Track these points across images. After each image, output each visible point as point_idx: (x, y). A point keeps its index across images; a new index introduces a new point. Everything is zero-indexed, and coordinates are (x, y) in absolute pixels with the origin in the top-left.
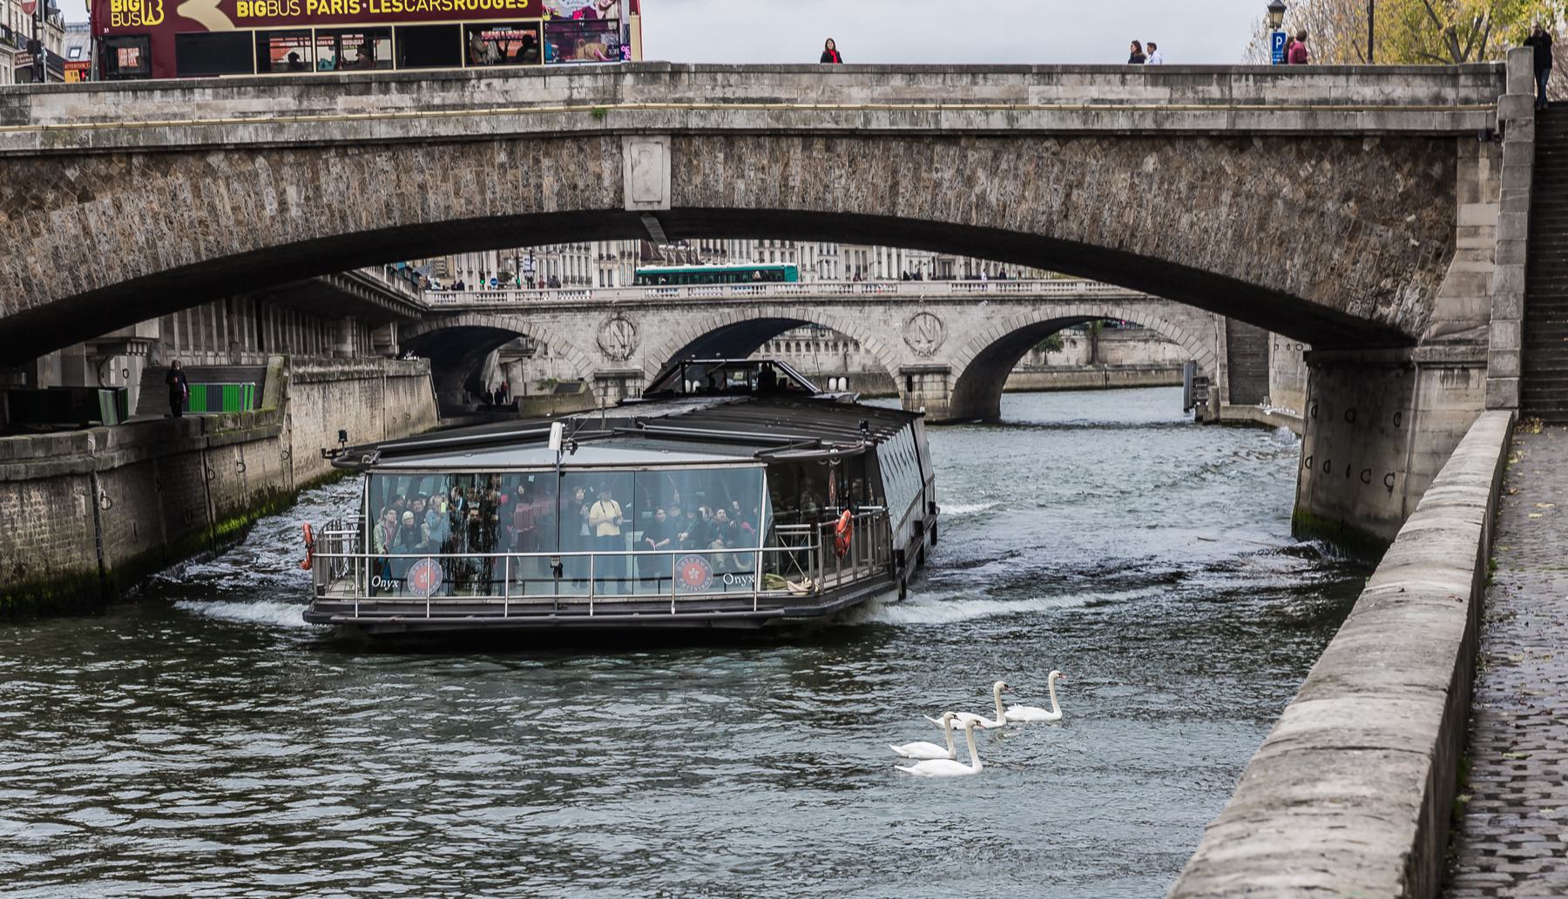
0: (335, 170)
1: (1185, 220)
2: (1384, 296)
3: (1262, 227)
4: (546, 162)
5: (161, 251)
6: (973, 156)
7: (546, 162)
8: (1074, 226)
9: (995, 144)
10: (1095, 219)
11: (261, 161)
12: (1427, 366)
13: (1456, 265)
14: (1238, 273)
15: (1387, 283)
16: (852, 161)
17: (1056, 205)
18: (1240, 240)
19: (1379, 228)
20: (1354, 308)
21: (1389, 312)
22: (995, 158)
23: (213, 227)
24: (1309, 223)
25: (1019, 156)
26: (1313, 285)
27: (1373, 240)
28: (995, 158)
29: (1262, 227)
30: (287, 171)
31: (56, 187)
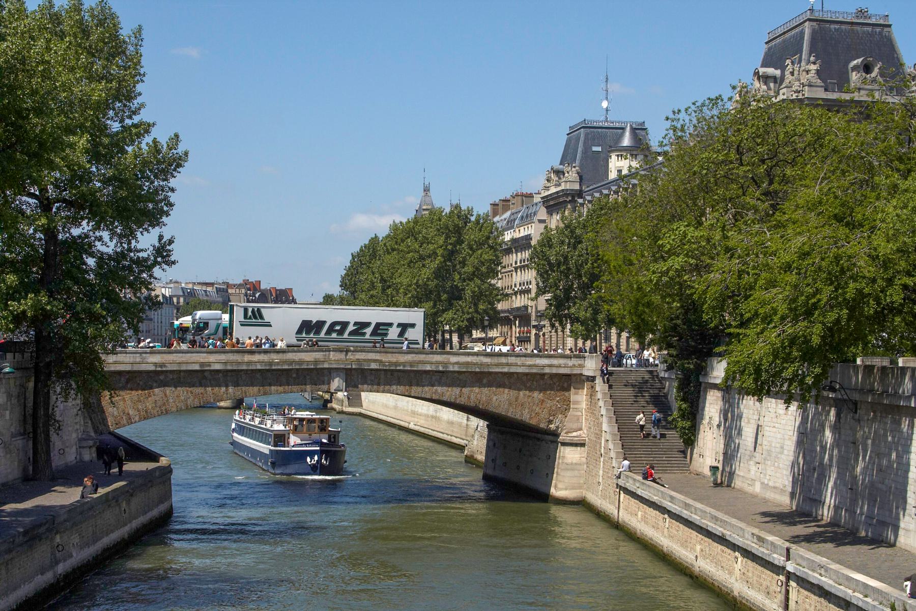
0: (243, 378)
1: (495, 398)
2: (550, 422)
3: (516, 401)
4: (308, 377)
5: (189, 402)
6: (434, 378)
7: (308, 377)
8: (463, 399)
9: (441, 374)
10: (469, 397)
11: (221, 375)
12: (564, 444)
13: (571, 412)
14: (509, 414)
15: (551, 418)
16: (399, 379)
17: (458, 393)
18: (510, 404)
19: (549, 401)
20: (543, 425)
21: (552, 426)
22: (440, 379)
23: (205, 395)
24: (530, 400)
25: (447, 378)
26: (531, 418)
27: (548, 405)
28: (440, 379)
29: (516, 401)
30: (229, 378)
31: (156, 382)
